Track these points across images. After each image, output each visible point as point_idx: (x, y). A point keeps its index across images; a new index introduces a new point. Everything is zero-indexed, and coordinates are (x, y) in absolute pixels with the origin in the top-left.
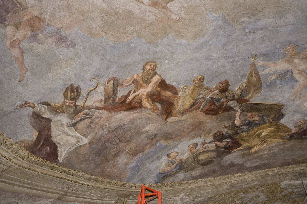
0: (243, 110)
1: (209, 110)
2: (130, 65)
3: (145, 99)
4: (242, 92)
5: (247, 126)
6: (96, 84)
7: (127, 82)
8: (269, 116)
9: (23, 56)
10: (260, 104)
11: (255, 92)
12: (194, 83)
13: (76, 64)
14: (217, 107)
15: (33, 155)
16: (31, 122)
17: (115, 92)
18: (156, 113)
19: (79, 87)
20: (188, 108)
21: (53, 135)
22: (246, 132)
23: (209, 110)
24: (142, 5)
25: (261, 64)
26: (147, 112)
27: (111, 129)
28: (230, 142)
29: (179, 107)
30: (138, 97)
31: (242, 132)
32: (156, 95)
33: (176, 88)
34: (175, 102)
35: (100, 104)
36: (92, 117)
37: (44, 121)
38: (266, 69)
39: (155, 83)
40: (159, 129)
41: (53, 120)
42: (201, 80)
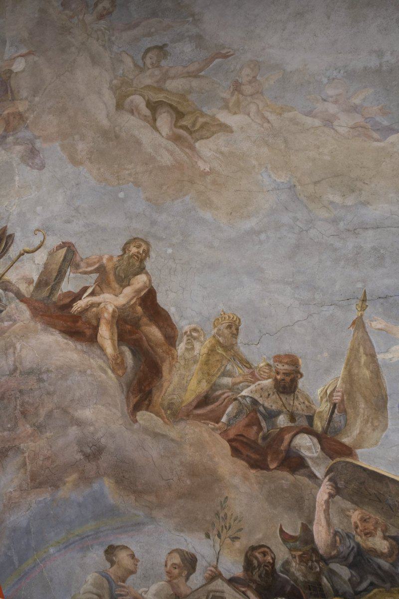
0: (336, 483)
1: (241, 438)
4: (333, 412)
5: (351, 566)
7: (89, 265)
10: (389, 478)
11: (369, 424)
12: (216, 330)
14: (264, 438)
17: (61, 275)
18: (118, 377)
20: (190, 404)
23: (241, 438)
25: (379, 326)
26: (100, 362)
27: (21, 363)
29: (172, 387)
30: (94, 309)
32: (131, 325)
34: (165, 368)
35: (27, 289)
42: (234, 328)
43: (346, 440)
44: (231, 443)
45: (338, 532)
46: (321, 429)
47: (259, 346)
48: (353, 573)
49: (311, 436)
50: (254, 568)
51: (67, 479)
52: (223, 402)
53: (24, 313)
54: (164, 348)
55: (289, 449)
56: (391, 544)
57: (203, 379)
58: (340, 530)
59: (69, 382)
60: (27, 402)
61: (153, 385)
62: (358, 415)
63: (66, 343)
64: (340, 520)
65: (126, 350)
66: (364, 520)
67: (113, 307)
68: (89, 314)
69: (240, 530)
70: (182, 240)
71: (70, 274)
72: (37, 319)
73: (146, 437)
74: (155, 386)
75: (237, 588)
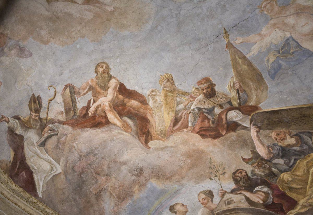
0: (257, 125)
1: (202, 129)
4: (239, 94)
5: (282, 157)
6: (54, 92)
7: (84, 89)
8: (309, 133)
10: (280, 110)
11: (259, 90)
12: (162, 86)
14: (213, 123)
15: (12, 181)
16: (8, 140)
17: (74, 102)
18: (129, 132)
19: (39, 96)
20: (170, 126)
21: (26, 156)
22: (289, 173)
23: (202, 129)
24: (77, 5)
25: (240, 41)
26: (117, 131)
27: (82, 152)
28: (268, 192)
29: (157, 124)
30: (100, 108)
31: (282, 172)
32: (121, 106)
34: (149, 117)
36: (57, 135)
37: (17, 138)
38: (251, 47)
39: (114, 89)
42: (170, 80)
43: (252, 104)
44: (199, 133)
45: (269, 146)
46: (237, 104)
47: (187, 82)
48: (285, 159)
49: (234, 110)
50: (239, 181)
51: (134, 190)
52: (185, 117)
53: (68, 129)
55: (227, 122)
56: (296, 138)
57: (170, 111)
58: (269, 145)
59: (109, 148)
60: (96, 167)
61: (148, 127)
62: (251, 89)
63: (96, 131)
64: (267, 140)
65: (125, 118)
66: (278, 135)
67: (108, 102)
68: (99, 112)
69: (224, 169)
71: (78, 99)
72: (76, 128)
73: (159, 152)
74: (149, 128)
75: (237, 193)
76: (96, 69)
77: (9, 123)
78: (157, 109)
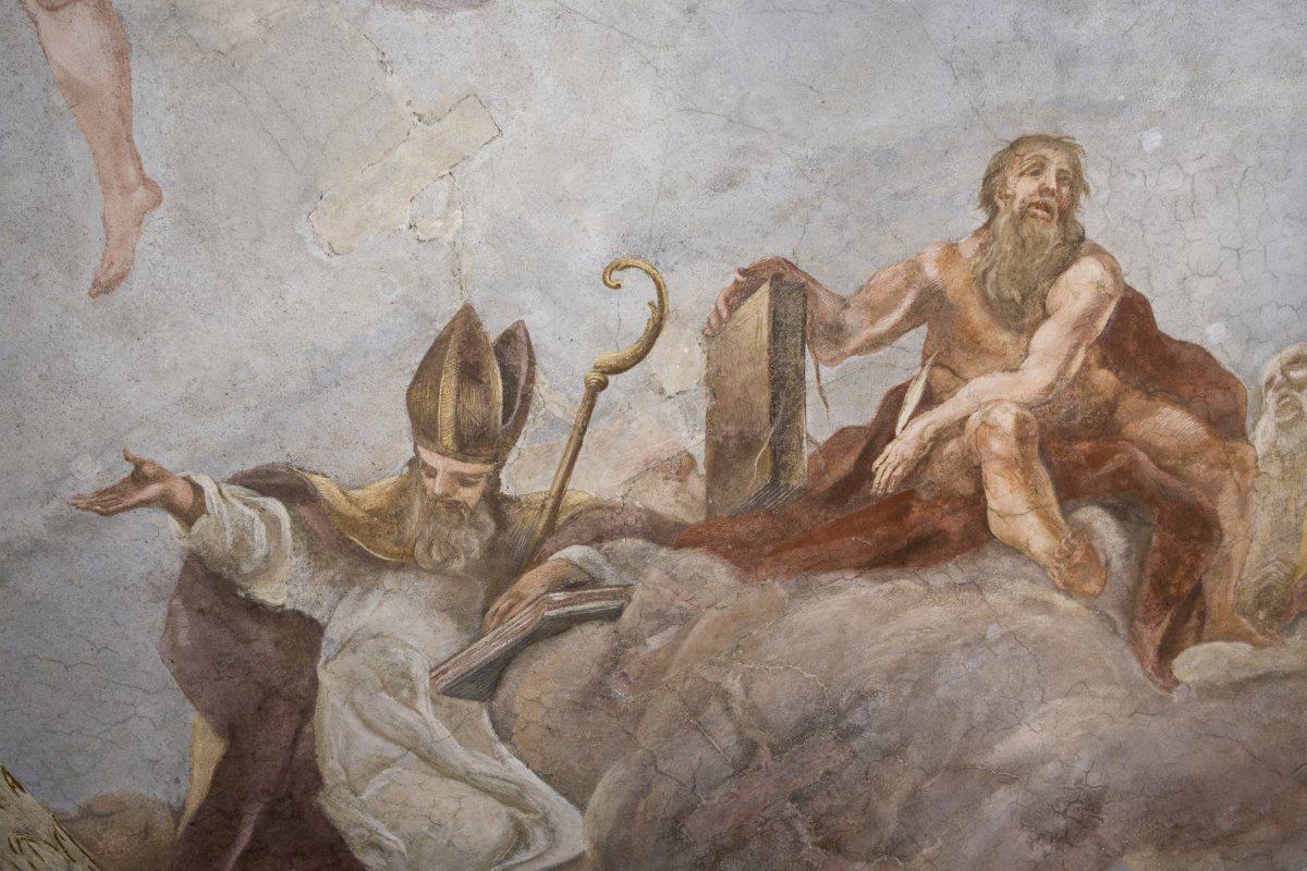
2: (887, 158)
3: (1010, 464)
6: (649, 310)
7: (877, 311)
9: (124, 75)
13: (497, 143)
16: (174, 647)
17: (785, 389)
18: (1090, 600)
19: (520, 333)
21: (331, 767)
26: (1021, 588)
27: (763, 725)
29: (1256, 548)
30: (952, 446)
32: (1089, 439)
33: (1231, 376)
34: (1226, 507)
35: (684, 497)
36: (614, 615)
37: (264, 640)
39: (1075, 328)
40: (1116, 751)
41: (334, 632)
54: (1210, 455)
59: (941, 692)
60: (830, 812)
61: (1202, 570)
67: (1014, 409)
70: (1190, 85)
71: (819, 372)
72: (763, 573)
76: (994, 174)
77: (202, 521)
78: (1287, 464)
